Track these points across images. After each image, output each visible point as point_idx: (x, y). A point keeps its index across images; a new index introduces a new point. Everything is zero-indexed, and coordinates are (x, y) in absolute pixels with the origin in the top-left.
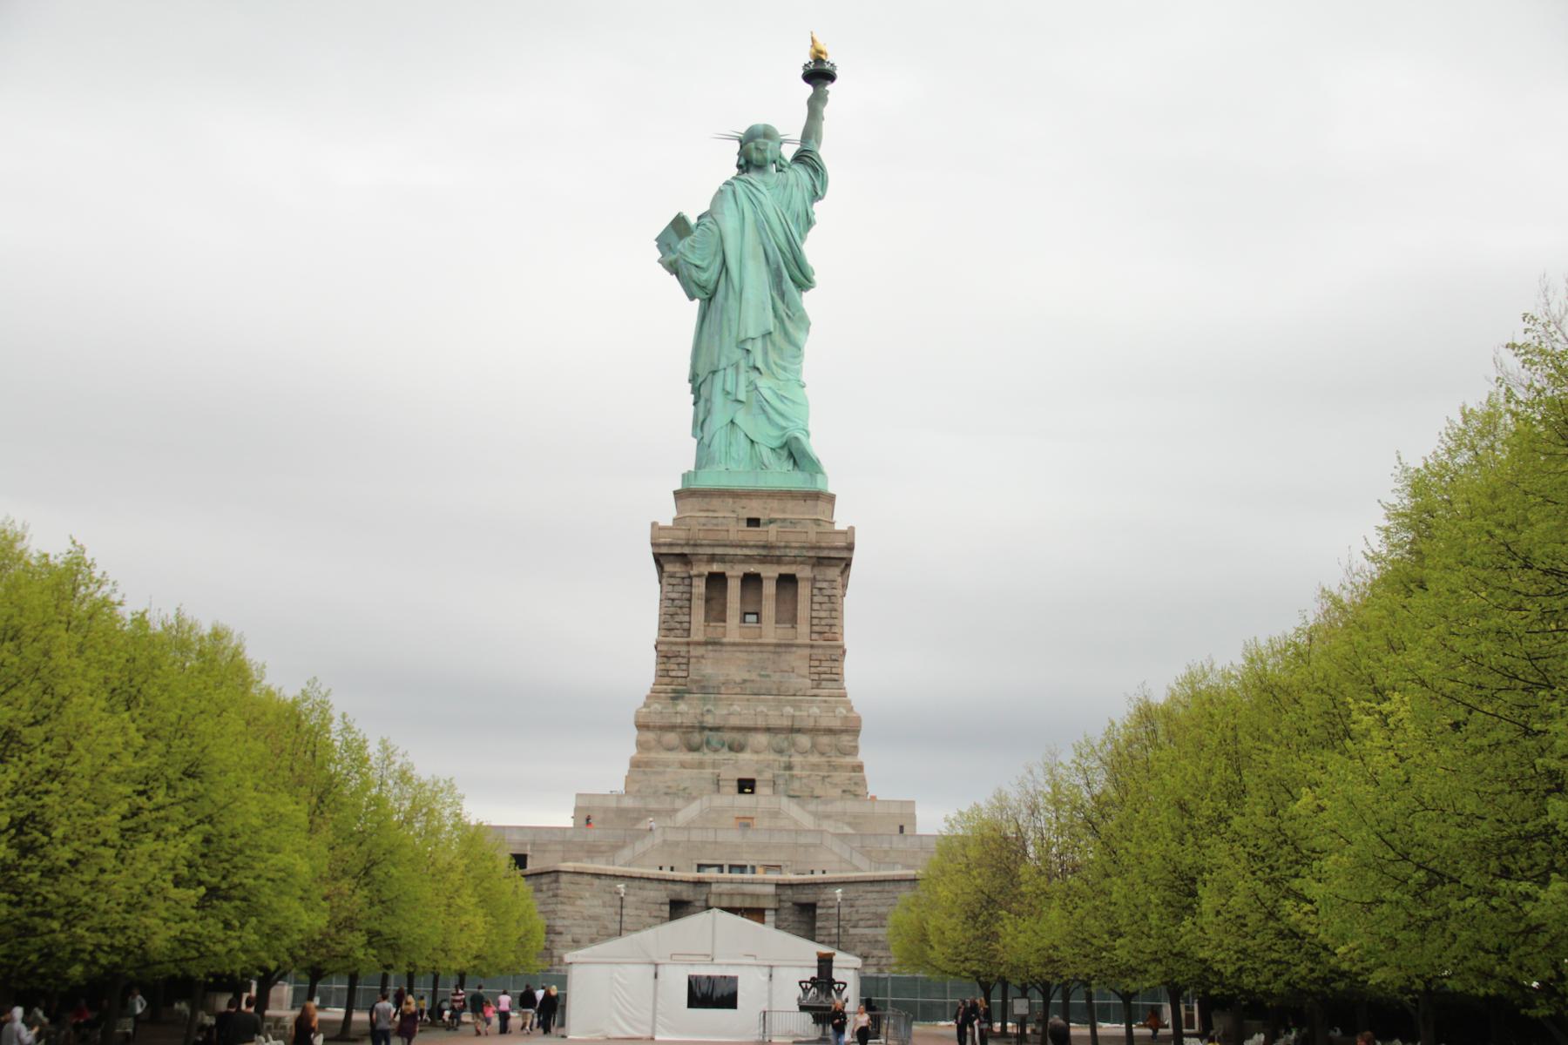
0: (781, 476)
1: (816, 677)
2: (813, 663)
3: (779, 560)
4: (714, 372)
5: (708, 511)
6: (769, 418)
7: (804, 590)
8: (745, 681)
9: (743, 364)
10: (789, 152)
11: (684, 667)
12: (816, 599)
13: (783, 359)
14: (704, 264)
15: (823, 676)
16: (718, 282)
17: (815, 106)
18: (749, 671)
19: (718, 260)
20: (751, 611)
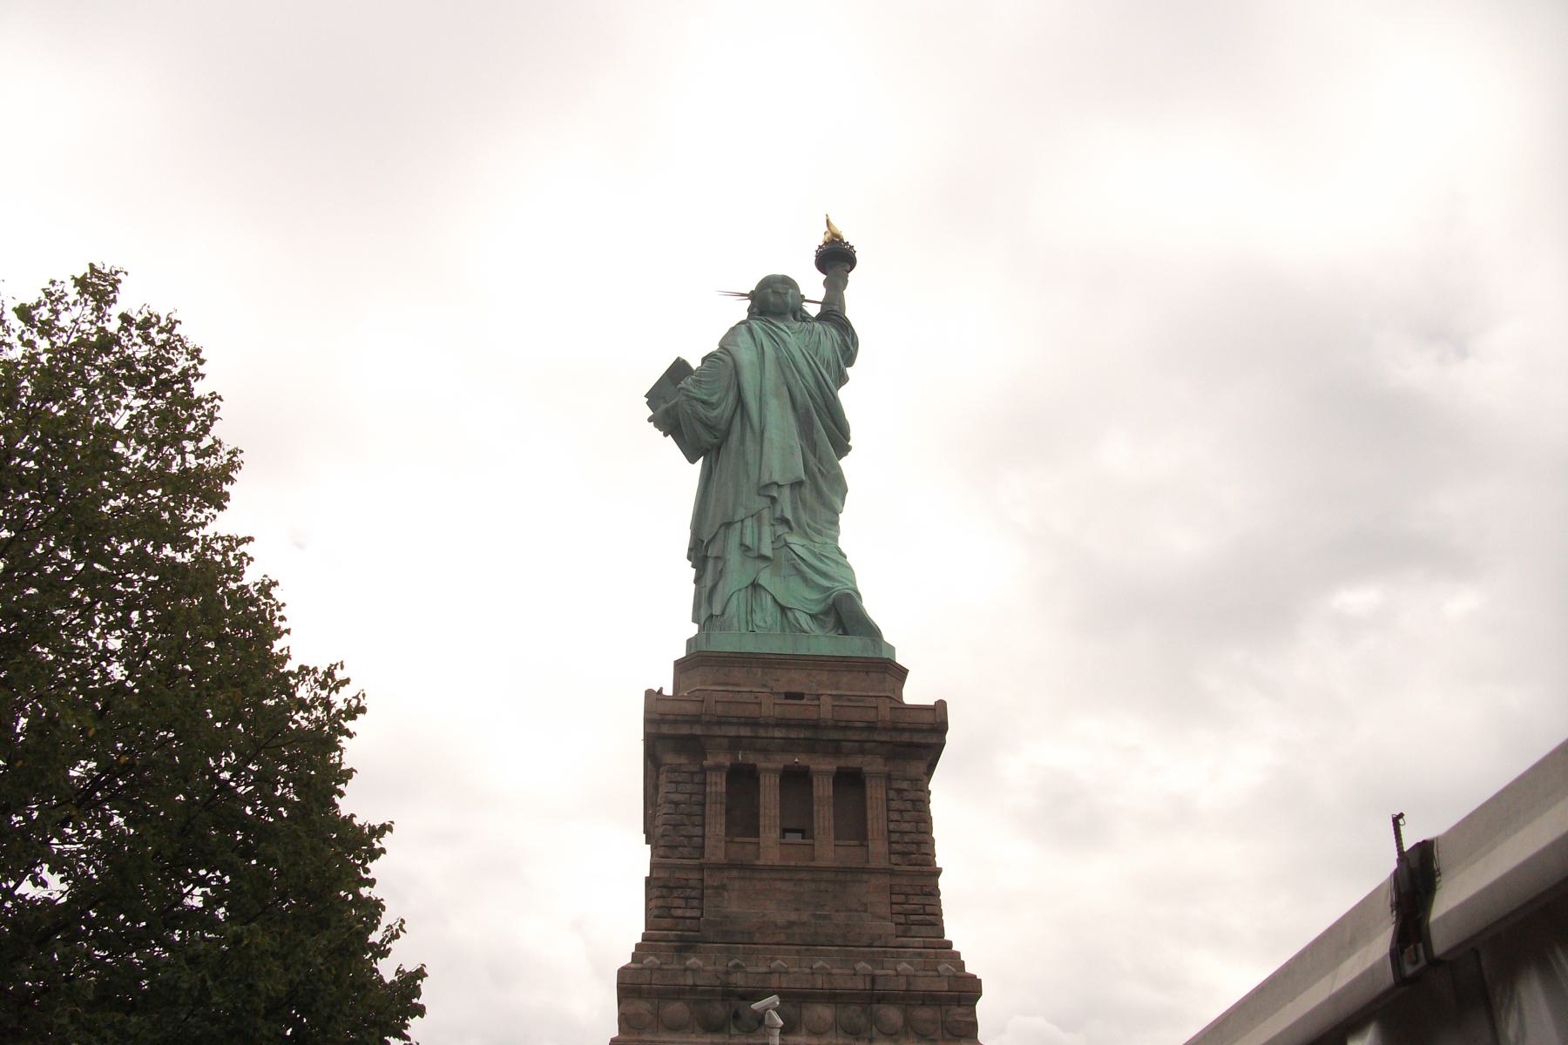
0: (825, 643)
1: (902, 919)
2: (896, 898)
3: (836, 749)
4: (728, 525)
5: (727, 684)
6: (805, 580)
7: (875, 793)
8: (791, 924)
9: (766, 514)
11: (695, 903)
12: (894, 805)
13: (815, 522)
14: (714, 399)
15: (913, 917)
16: (730, 422)
18: (797, 910)
19: (731, 398)
20: (798, 826)
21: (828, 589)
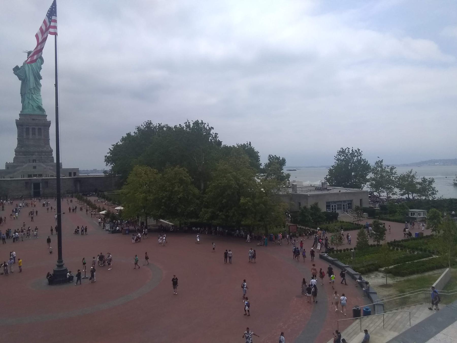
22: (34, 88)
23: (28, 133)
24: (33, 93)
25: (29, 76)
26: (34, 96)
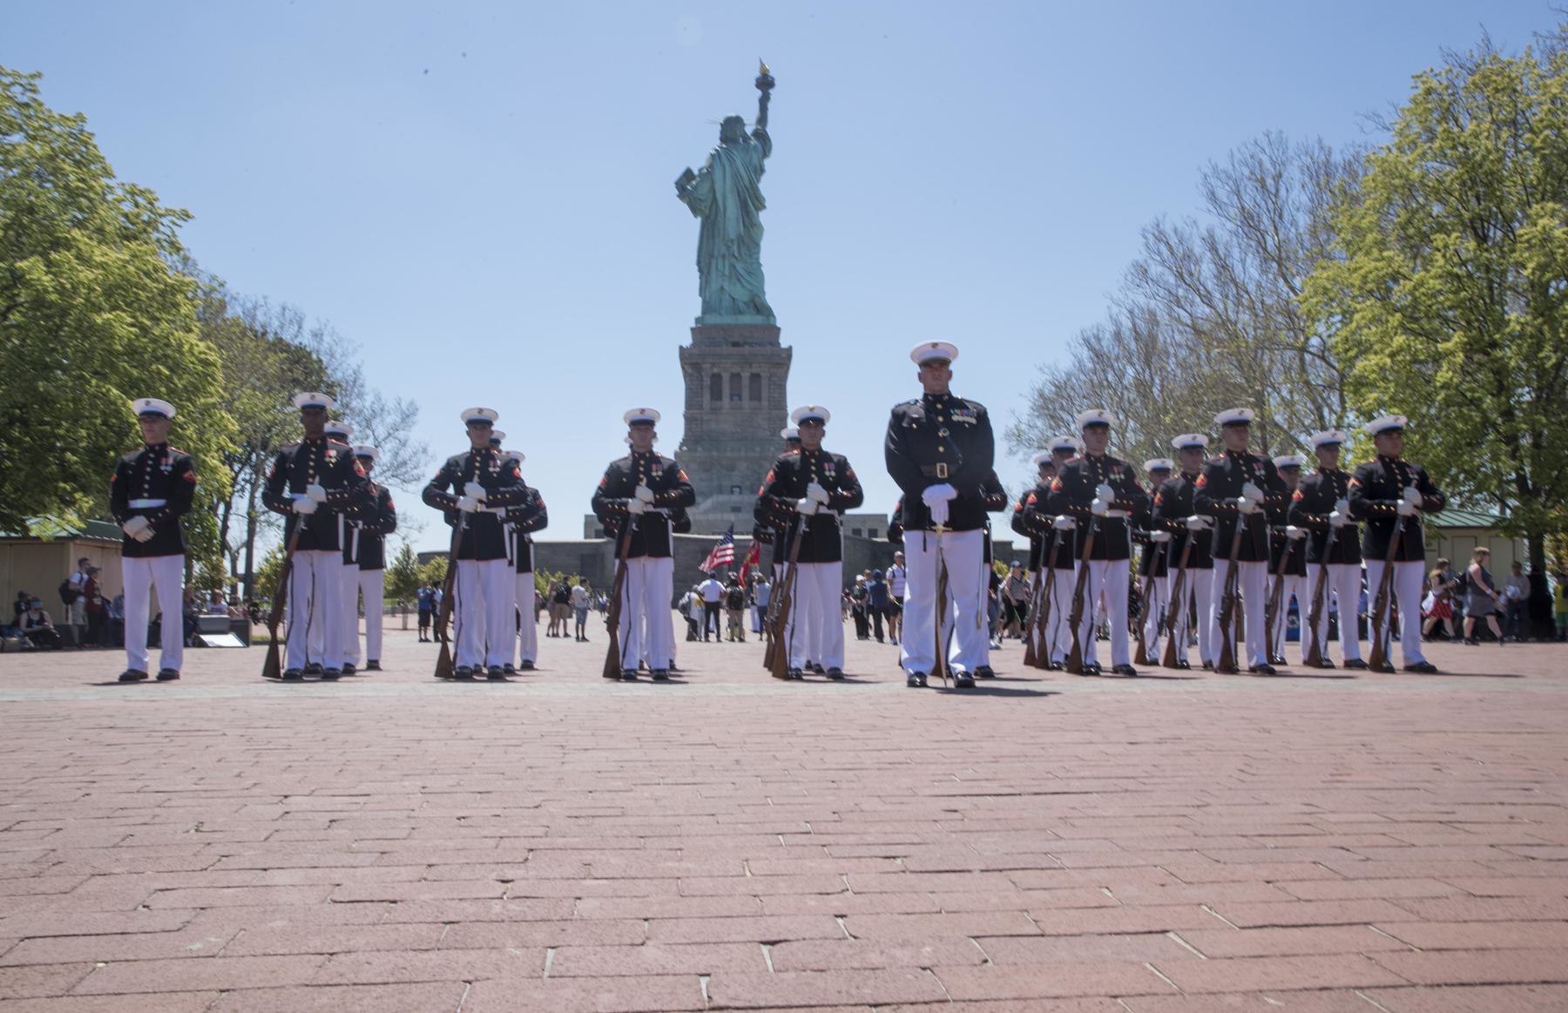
6: (743, 286)
10: (749, 130)
14: (702, 198)
17: (764, 102)
21: (751, 291)
22: (740, 239)
23: (716, 394)
24: (736, 254)
25: (724, 198)
26: (739, 266)
